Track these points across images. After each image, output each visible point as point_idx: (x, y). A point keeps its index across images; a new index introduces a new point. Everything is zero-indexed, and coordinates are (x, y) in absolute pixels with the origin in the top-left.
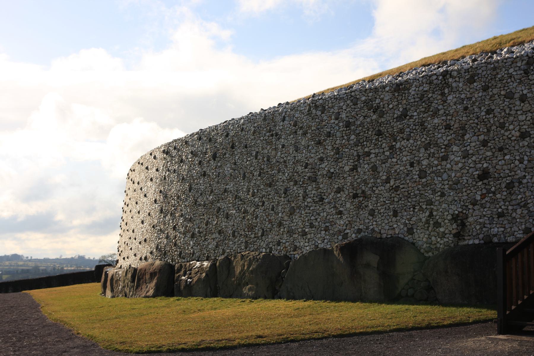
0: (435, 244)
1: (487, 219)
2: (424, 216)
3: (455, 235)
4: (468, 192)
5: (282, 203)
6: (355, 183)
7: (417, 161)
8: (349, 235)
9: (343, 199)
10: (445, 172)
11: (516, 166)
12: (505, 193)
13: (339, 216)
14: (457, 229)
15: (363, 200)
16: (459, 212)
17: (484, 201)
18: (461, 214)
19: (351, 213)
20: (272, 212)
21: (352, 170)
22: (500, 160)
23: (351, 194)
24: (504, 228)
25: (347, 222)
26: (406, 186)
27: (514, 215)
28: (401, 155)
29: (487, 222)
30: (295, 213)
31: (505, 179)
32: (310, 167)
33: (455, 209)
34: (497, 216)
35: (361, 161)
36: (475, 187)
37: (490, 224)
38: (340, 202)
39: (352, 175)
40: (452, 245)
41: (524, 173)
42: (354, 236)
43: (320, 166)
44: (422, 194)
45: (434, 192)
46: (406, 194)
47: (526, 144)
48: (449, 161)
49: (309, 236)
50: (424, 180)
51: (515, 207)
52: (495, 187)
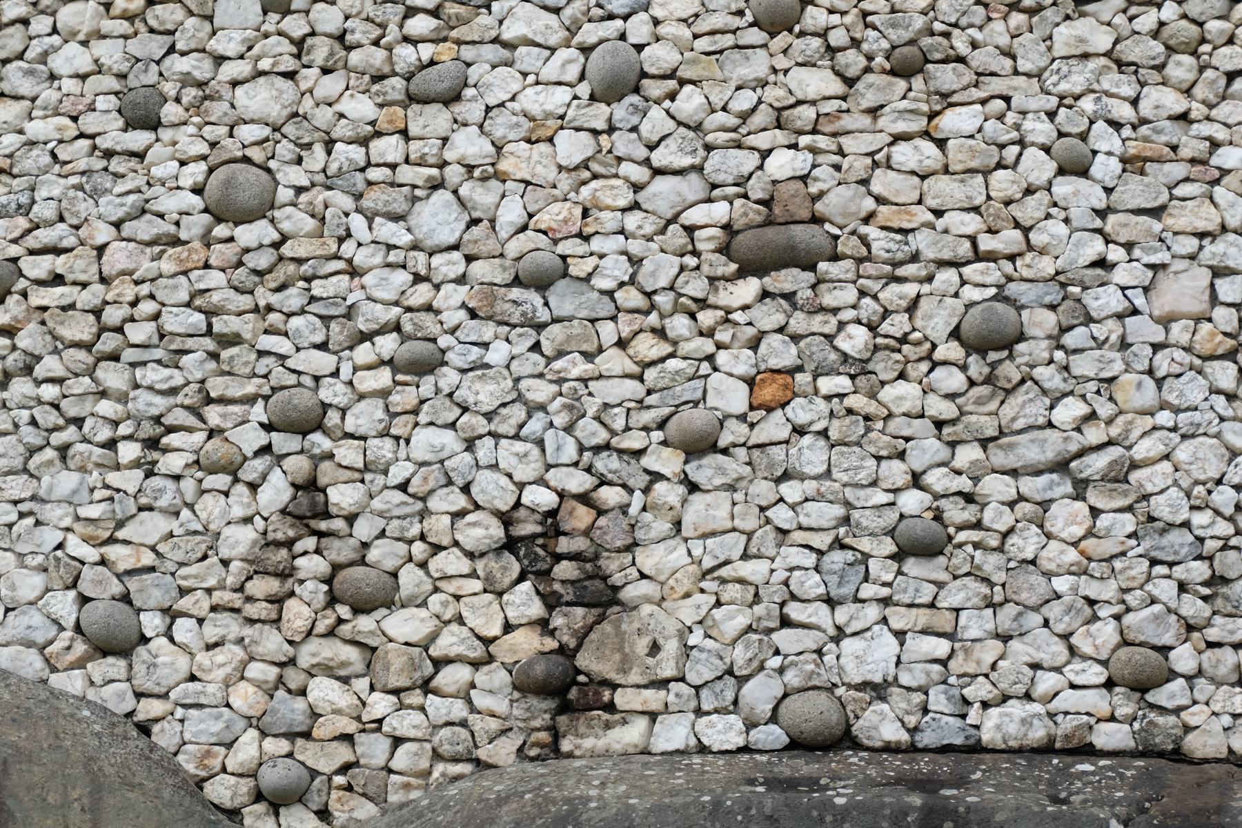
0: (347, 738)
1: (810, 560)
2: (236, 522)
3: (524, 686)
4: (647, 347)
7: (187, 80)
10: (436, 185)
11: (1029, 191)
12: (956, 381)
14: (543, 625)
16: (561, 495)
17: (774, 427)
18: (582, 516)
22: (897, 138)
24: (951, 636)
26: (78, 265)
27: (1026, 543)
28: (41, 24)
29: (811, 584)
31: (947, 277)
33: (516, 474)
34: (889, 547)
36: (707, 318)
37: (831, 602)
40: (503, 752)
41: (1095, 247)
44: (234, 340)
45: (345, 330)
46: (81, 328)
47: (1103, 41)
48: (471, 110)
50: (247, 234)
51: (1032, 486)
52: (872, 328)
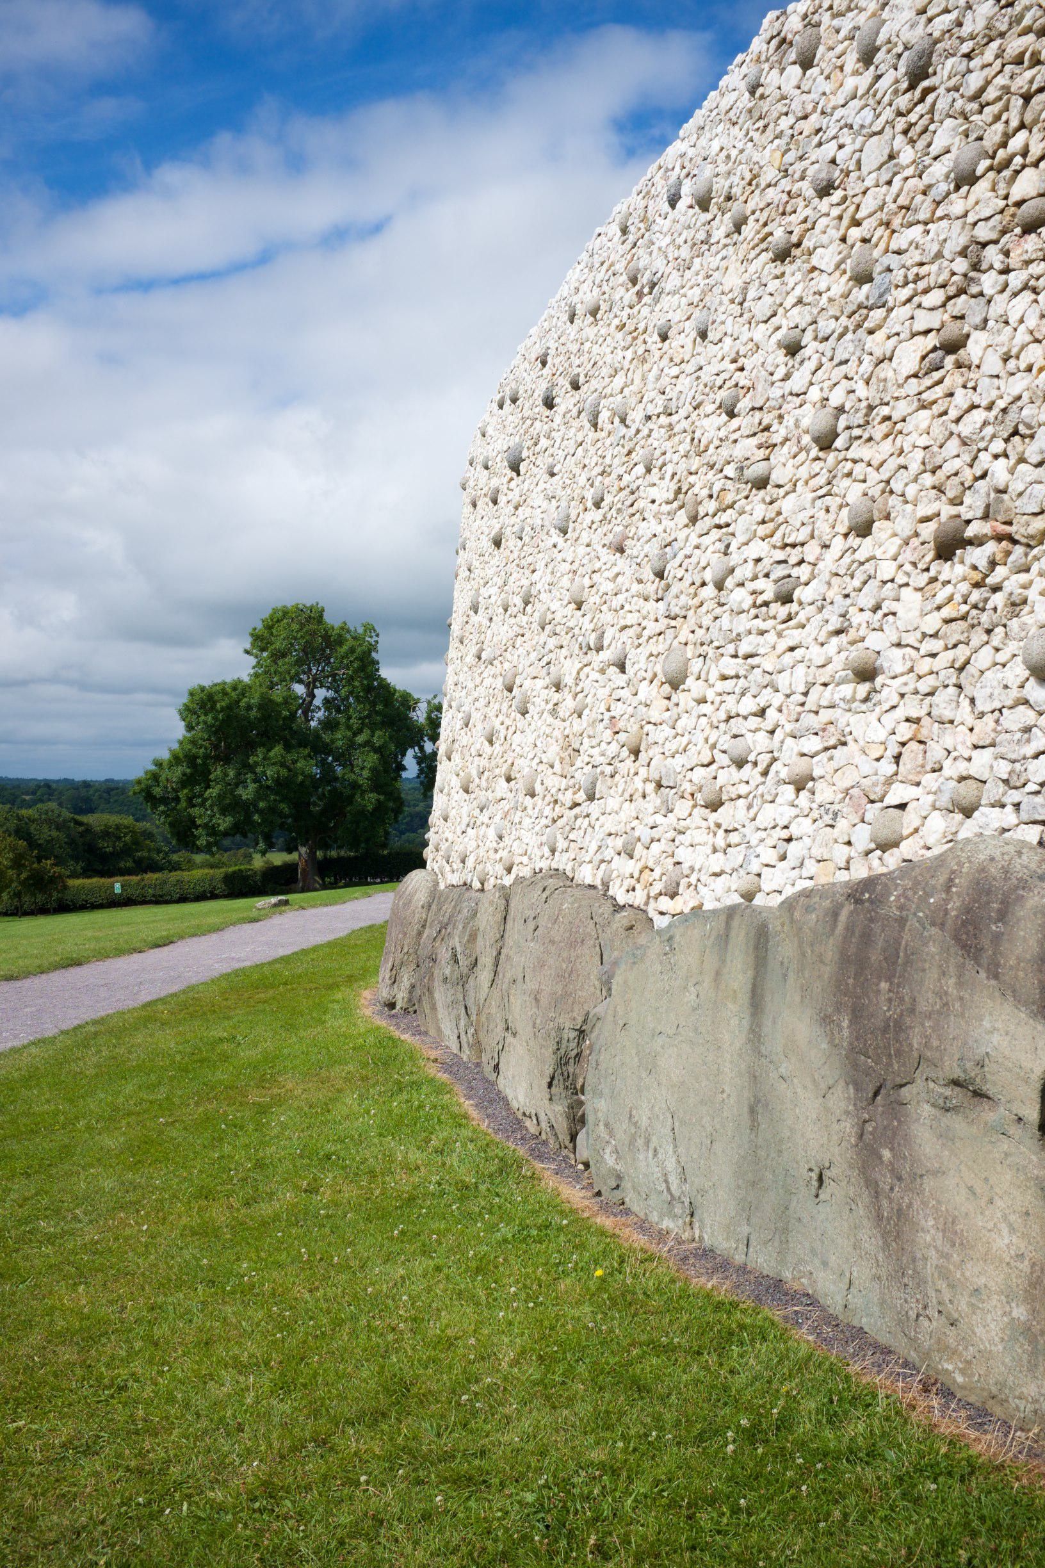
5: (652, 628)
6: (953, 445)
8: (910, 819)
9: (887, 569)
13: (863, 689)
15: (993, 564)
19: (924, 665)
20: (621, 680)
21: (930, 366)
23: (928, 531)
25: (905, 731)
30: (688, 681)
32: (743, 405)
35: (989, 282)
38: (866, 599)
39: (939, 391)
42: (938, 824)
43: (789, 386)
49: (724, 815)
